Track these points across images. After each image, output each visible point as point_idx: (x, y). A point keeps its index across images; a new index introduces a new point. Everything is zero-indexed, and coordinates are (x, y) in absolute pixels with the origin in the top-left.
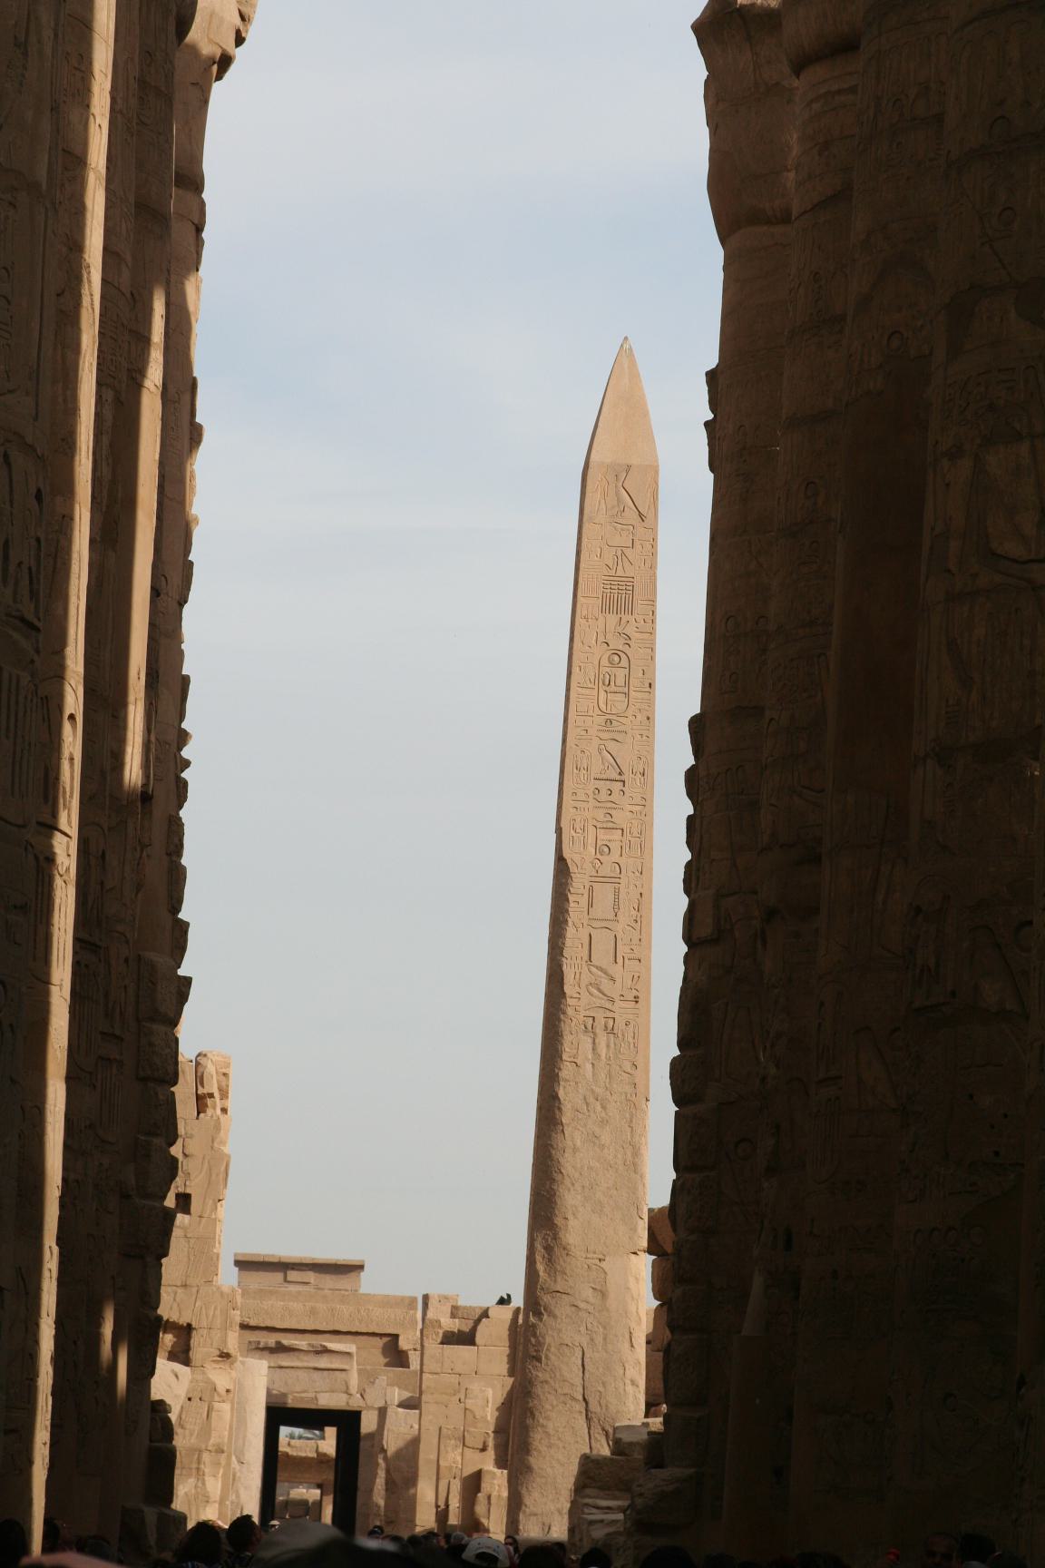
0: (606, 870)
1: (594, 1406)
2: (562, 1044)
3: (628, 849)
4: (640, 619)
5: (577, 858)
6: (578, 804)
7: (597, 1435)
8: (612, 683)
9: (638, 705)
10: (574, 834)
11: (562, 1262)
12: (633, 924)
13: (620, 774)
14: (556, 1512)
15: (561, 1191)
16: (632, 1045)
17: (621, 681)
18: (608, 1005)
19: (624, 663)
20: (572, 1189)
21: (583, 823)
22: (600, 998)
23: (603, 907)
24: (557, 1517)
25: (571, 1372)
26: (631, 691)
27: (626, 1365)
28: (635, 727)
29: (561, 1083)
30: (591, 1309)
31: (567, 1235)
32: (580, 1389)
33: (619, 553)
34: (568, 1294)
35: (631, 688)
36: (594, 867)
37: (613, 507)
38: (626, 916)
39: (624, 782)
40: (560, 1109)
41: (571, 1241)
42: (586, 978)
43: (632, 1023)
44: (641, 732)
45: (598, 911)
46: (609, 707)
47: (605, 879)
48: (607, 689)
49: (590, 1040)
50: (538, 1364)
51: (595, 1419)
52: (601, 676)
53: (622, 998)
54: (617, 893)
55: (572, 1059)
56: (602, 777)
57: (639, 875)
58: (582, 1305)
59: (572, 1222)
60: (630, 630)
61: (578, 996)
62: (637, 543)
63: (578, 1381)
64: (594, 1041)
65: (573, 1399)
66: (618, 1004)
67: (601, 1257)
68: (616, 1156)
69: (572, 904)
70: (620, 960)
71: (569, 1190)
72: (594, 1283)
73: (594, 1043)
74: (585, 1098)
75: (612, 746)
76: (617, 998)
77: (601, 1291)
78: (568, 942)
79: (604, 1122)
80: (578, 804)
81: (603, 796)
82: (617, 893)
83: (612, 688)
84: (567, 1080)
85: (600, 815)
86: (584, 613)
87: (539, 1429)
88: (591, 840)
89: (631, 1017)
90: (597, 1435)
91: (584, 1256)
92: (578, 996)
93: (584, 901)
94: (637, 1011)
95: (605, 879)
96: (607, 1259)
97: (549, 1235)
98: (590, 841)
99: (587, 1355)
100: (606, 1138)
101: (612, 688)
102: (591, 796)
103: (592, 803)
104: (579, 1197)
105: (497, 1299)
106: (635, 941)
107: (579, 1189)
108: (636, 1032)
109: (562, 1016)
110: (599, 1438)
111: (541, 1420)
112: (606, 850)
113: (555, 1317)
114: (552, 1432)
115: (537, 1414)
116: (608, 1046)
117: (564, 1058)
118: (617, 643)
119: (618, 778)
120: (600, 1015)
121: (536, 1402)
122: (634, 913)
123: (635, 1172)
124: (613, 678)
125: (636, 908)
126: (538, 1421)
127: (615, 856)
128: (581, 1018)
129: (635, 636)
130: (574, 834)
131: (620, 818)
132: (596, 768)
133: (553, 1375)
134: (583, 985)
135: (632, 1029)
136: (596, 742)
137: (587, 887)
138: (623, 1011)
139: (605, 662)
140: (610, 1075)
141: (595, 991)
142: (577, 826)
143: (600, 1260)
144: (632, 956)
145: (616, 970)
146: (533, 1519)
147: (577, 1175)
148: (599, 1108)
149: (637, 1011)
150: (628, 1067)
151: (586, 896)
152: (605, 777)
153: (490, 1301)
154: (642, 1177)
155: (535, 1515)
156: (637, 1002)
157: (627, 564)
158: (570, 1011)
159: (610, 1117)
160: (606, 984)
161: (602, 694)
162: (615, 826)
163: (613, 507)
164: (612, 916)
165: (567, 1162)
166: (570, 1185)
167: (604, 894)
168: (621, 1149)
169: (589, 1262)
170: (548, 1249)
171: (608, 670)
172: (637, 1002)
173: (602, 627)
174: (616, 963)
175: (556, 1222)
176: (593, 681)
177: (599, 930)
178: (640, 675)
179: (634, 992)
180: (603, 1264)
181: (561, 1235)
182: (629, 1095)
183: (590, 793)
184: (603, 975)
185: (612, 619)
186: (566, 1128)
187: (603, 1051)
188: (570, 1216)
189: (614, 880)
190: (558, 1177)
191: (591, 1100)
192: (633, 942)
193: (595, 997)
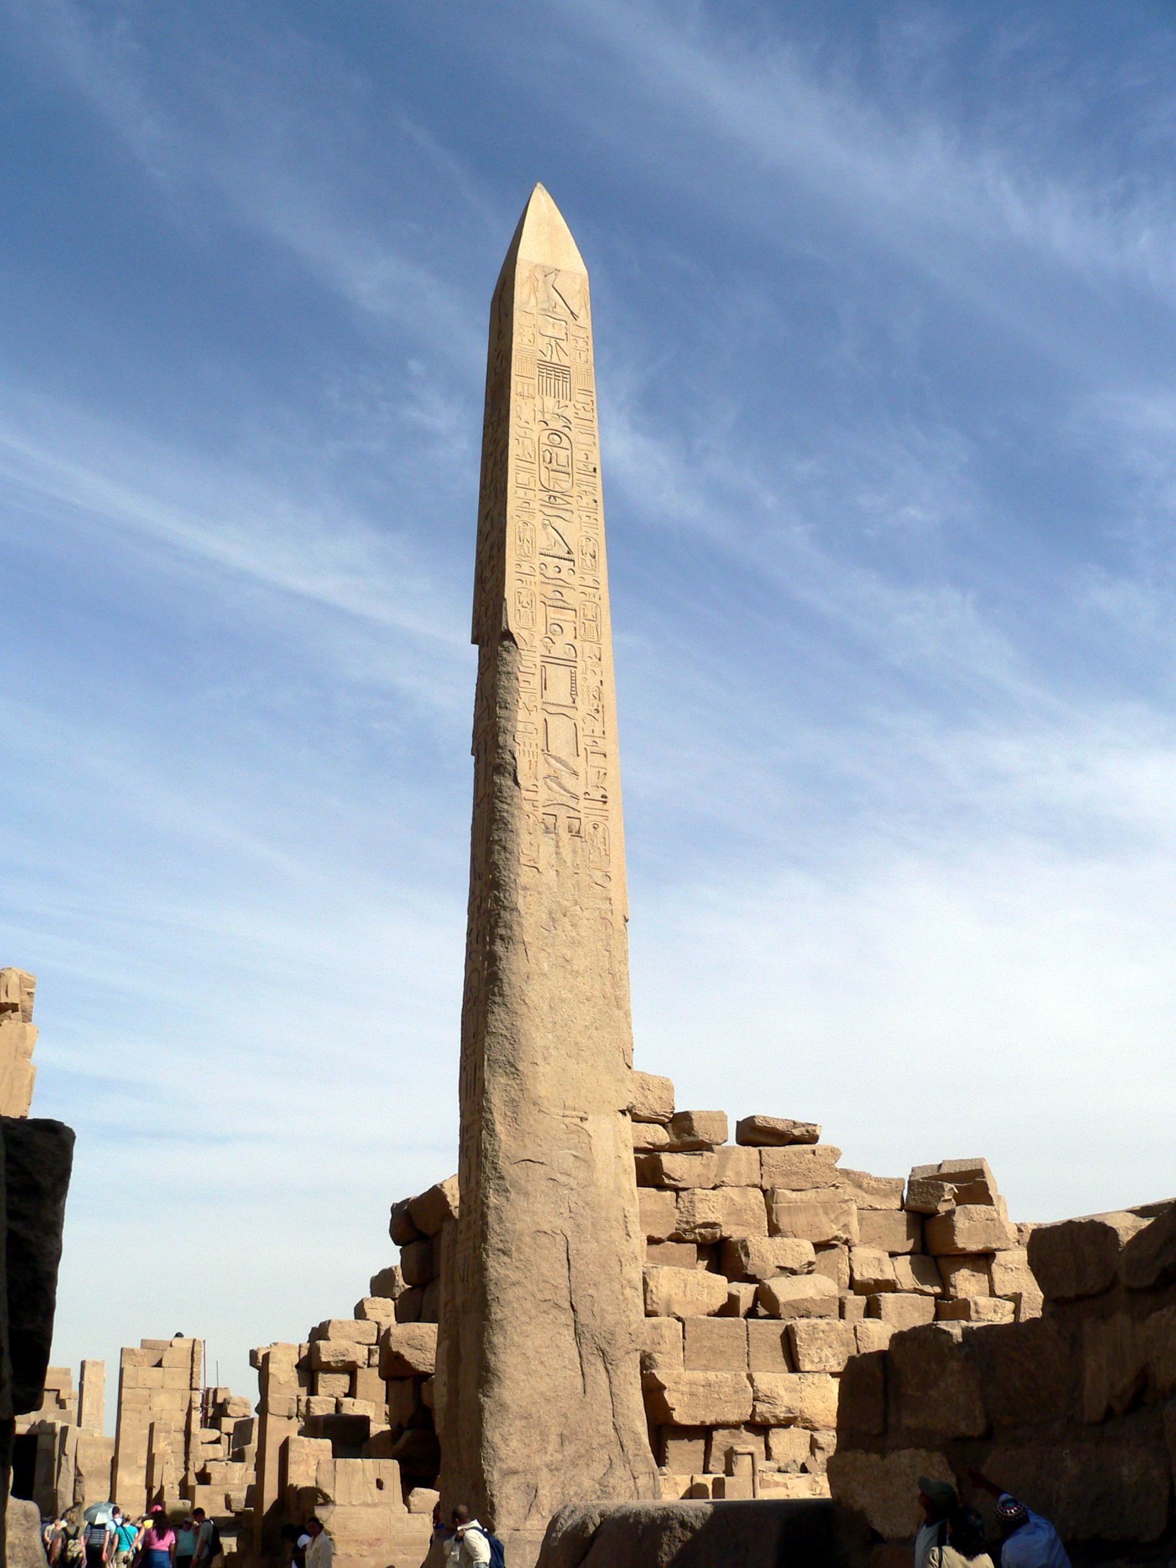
0: (559, 650)
1: (583, 1317)
2: (519, 845)
3: (582, 632)
4: (579, 406)
5: (525, 634)
6: (524, 577)
7: (590, 1358)
8: (554, 461)
9: (584, 488)
10: (521, 608)
11: (532, 1122)
12: (596, 715)
13: (568, 553)
14: (543, 1467)
15: (527, 1027)
16: (603, 853)
17: (563, 461)
18: (572, 803)
19: (565, 443)
20: (541, 1029)
21: (530, 598)
22: (563, 795)
23: (559, 690)
24: (545, 1474)
25: (551, 1266)
26: (575, 474)
27: (622, 1260)
28: (580, 508)
29: (520, 892)
30: (573, 1184)
31: (538, 1086)
32: (566, 1292)
33: (553, 343)
34: (542, 1163)
35: (575, 470)
36: (546, 647)
37: (544, 302)
38: (585, 706)
39: (573, 561)
40: (520, 924)
41: (543, 1093)
42: (543, 770)
43: (601, 827)
44: (589, 514)
45: (550, 696)
46: (552, 484)
47: (558, 662)
48: (548, 466)
49: (552, 843)
50: (506, 1259)
51: (588, 1335)
52: (541, 453)
53: (587, 796)
54: (573, 681)
55: (531, 864)
56: (547, 552)
57: (597, 661)
58: (563, 1179)
59: (543, 1068)
60: (569, 414)
61: (534, 788)
62: (571, 338)
63: (563, 1282)
64: (557, 842)
65: (557, 1306)
66: (582, 804)
67: (582, 1115)
68: (592, 987)
69: (522, 684)
70: (582, 752)
71: (537, 1028)
72: (576, 1148)
73: (557, 847)
74: (550, 913)
75: (558, 523)
76: (582, 797)
77: (585, 1161)
78: (520, 726)
79: (574, 943)
80: (524, 577)
81: (551, 572)
82: (573, 681)
83: (554, 466)
84: (525, 889)
85: (549, 591)
86: (520, 389)
87: (513, 1349)
88: (541, 620)
89: (600, 819)
90: (590, 1358)
91: (561, 1114)
92: (534, 788)
93: (536, 682)
94: (604, 813)
95: (558, 662)
96: (590, 1117)
97: (511, 1086)
98: (538, 616)
99: (571, 1246)
100: (580, 964)
101: (554, 466)
102: (538, 570)
103: (539, 578)
104: (550, 1036)
105: (174, 1334)
106: (598, 733)
107: (550, 1025)
108: (607, 837)
109: (516, 812)
110: (593, 1361)
111: (515, 1337)
112: (558, 629)
113: (527, 1194)
114: (530, 1353)
115: (509, 1328)
116: (574, 852)
117: (522, 861)
118: (558, 425)
119: (567, 556)
120: (562, 813)
121: (507, 1311)
122: (596, 702)
123: (619, 1008)
124: (554, 455)
125: (597, 697)
126: (512, 1339)
127: (569, 636)
128: (540, 815)
129: (574, 421)
130: (521, 608)
131: (571, 597)
132: (542, 542)
133: (528, 1274)
134: (540, 777)
135: (601, 833)
136: (540, 516)
137: (539, 666)
138: (587, 811)
139: (544, 439)
140: (577, 885)
141: (554, 786)
142: (524, 599)
143: (582, 1119)
144: (595, 749)
145: (579, 764)
146: (514, 1480)
147: (546, 1008)
148: (568, 927)
149: (604, 813)
150: (598, 876)
151: (538, 676)
152: (552, 553)
153: (170, 1337)
154: (627, 1014)
155: (516, 1472)
156: (605, 802)
157: (561, 353)
158: (527, 807)
159: (582, 937)
160: (567, 780)
161: (544, 471)
162: (566, 605)
163: (544, 302)
164: (569, 702)
165: (533, 990)
166: (537, 1020)
167: (559, 678)
168: (599, 977)
169: (567, 1120)
170: (513, 1103)
171: (549, 448)
172: (605, 802)
173: (539, 407)
174: (578, 755)
175: (520, 1068)
176: (533, 456)
177: (555, 717)
178: (583, 458)
179: (603, 792)
180: (585, 1125)
181: (529, 1084)
182: (603, 912)
183: (536, 566)
184: (565, 769)
185: (550, 403)
186: (528, 946)
187: (566, 853)
188: (540, 1061)
189: (569, 663)
190: (522, 1010)
191: (559, 915)
192: (595, 734)
193: (556, 793)
